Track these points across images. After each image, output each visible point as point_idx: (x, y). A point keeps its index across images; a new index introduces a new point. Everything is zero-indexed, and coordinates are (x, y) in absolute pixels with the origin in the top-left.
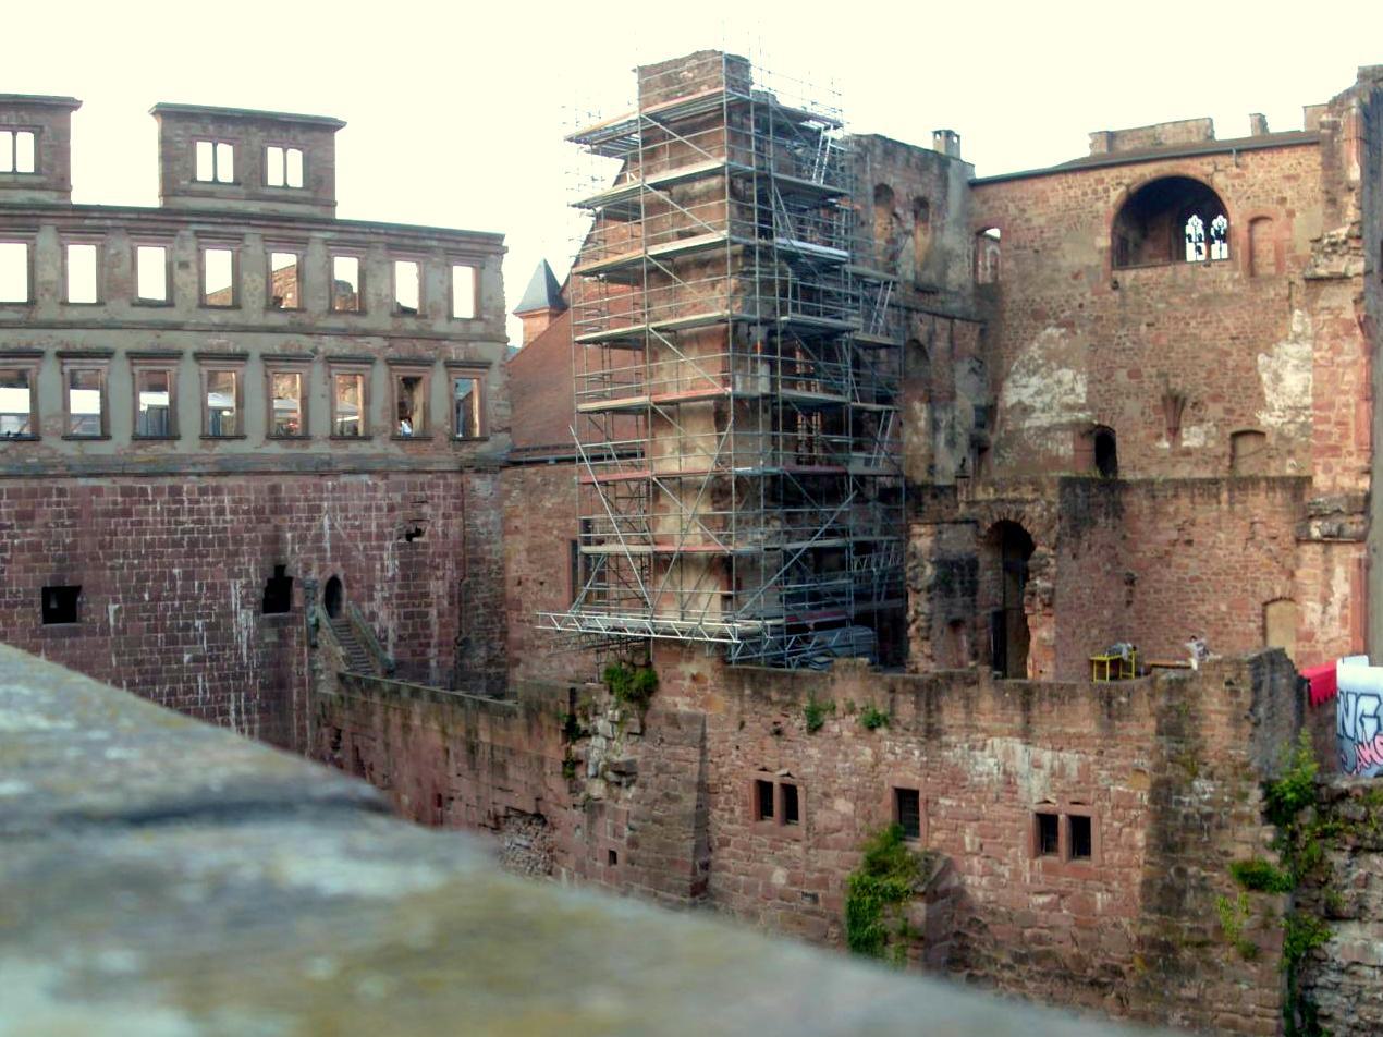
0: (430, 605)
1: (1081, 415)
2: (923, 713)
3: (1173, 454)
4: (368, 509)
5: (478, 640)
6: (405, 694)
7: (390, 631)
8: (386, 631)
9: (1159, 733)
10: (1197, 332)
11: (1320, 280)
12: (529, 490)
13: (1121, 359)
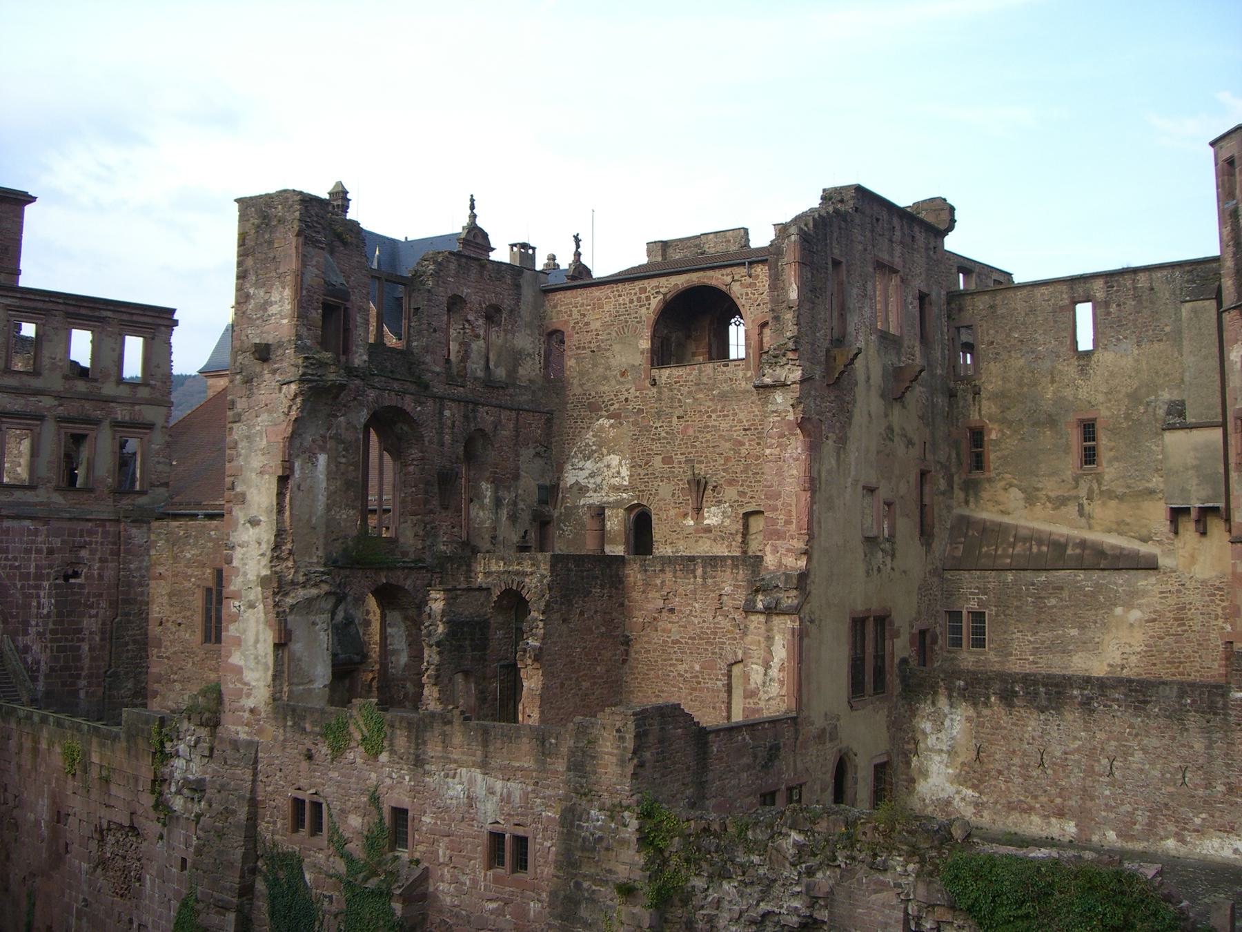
0: (83, 640)
1: (624, 495)
2: (413, 745)
3: (697, 531)
4: (28, 551)
5: (127, 673)
6: (36, 719)
7: (42, 663)
8: (38, 663)
9: (569, 769)
10: (716, 423)
11: (766, 387)
12: (173, 542)
13: (656, 447)
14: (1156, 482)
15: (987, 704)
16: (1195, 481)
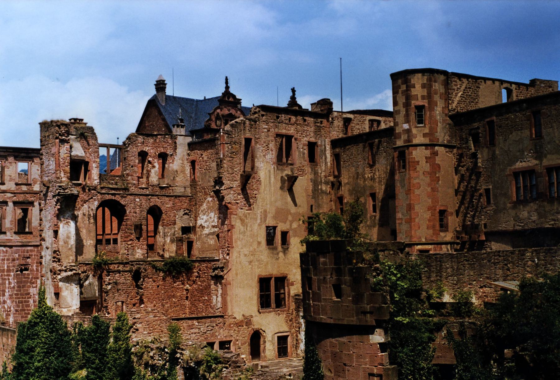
0: (30, 298)
7: (12, 309)
8: (10, 308)
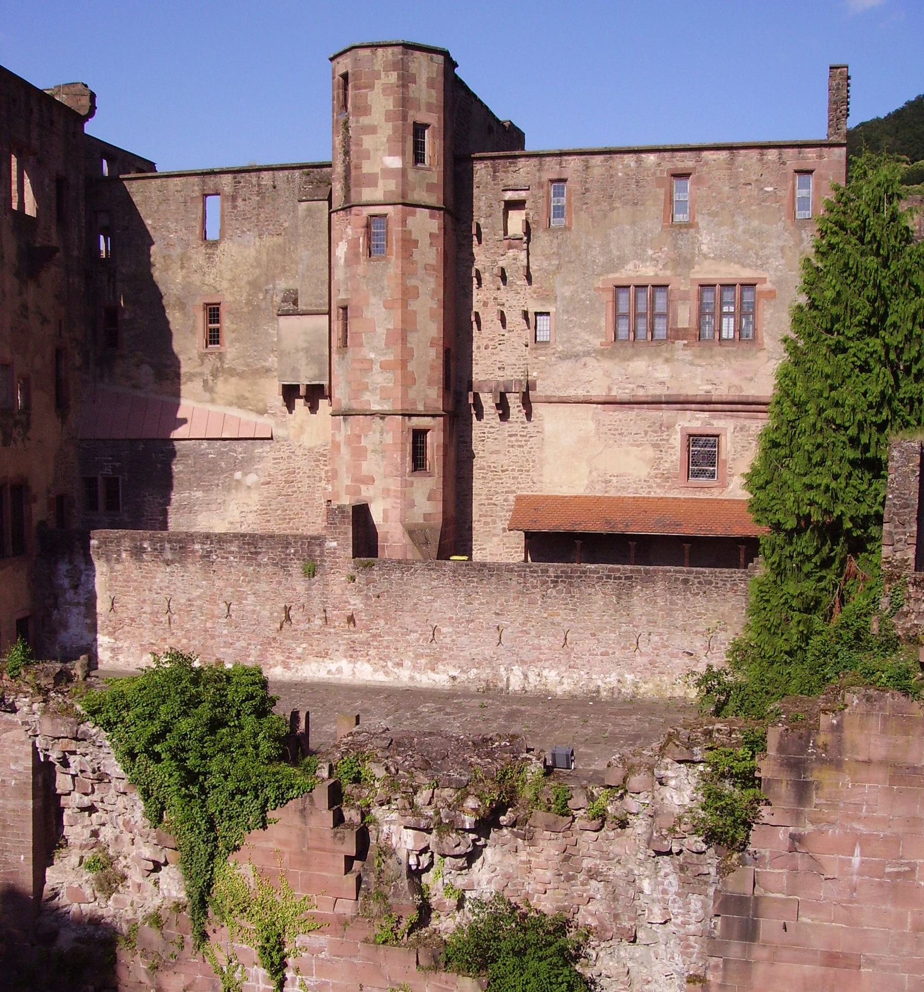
14: (272, 361)
15: (118, 561)
16: (304, 362)
